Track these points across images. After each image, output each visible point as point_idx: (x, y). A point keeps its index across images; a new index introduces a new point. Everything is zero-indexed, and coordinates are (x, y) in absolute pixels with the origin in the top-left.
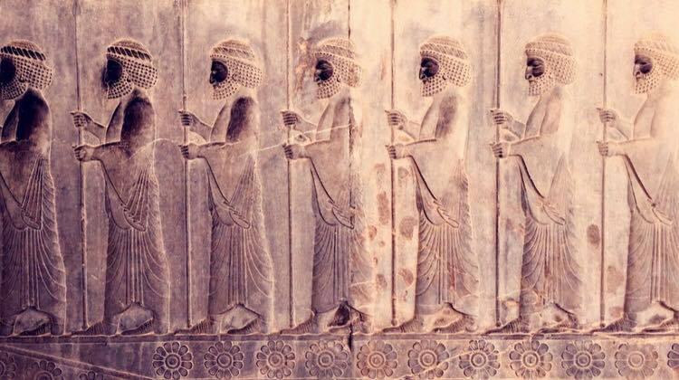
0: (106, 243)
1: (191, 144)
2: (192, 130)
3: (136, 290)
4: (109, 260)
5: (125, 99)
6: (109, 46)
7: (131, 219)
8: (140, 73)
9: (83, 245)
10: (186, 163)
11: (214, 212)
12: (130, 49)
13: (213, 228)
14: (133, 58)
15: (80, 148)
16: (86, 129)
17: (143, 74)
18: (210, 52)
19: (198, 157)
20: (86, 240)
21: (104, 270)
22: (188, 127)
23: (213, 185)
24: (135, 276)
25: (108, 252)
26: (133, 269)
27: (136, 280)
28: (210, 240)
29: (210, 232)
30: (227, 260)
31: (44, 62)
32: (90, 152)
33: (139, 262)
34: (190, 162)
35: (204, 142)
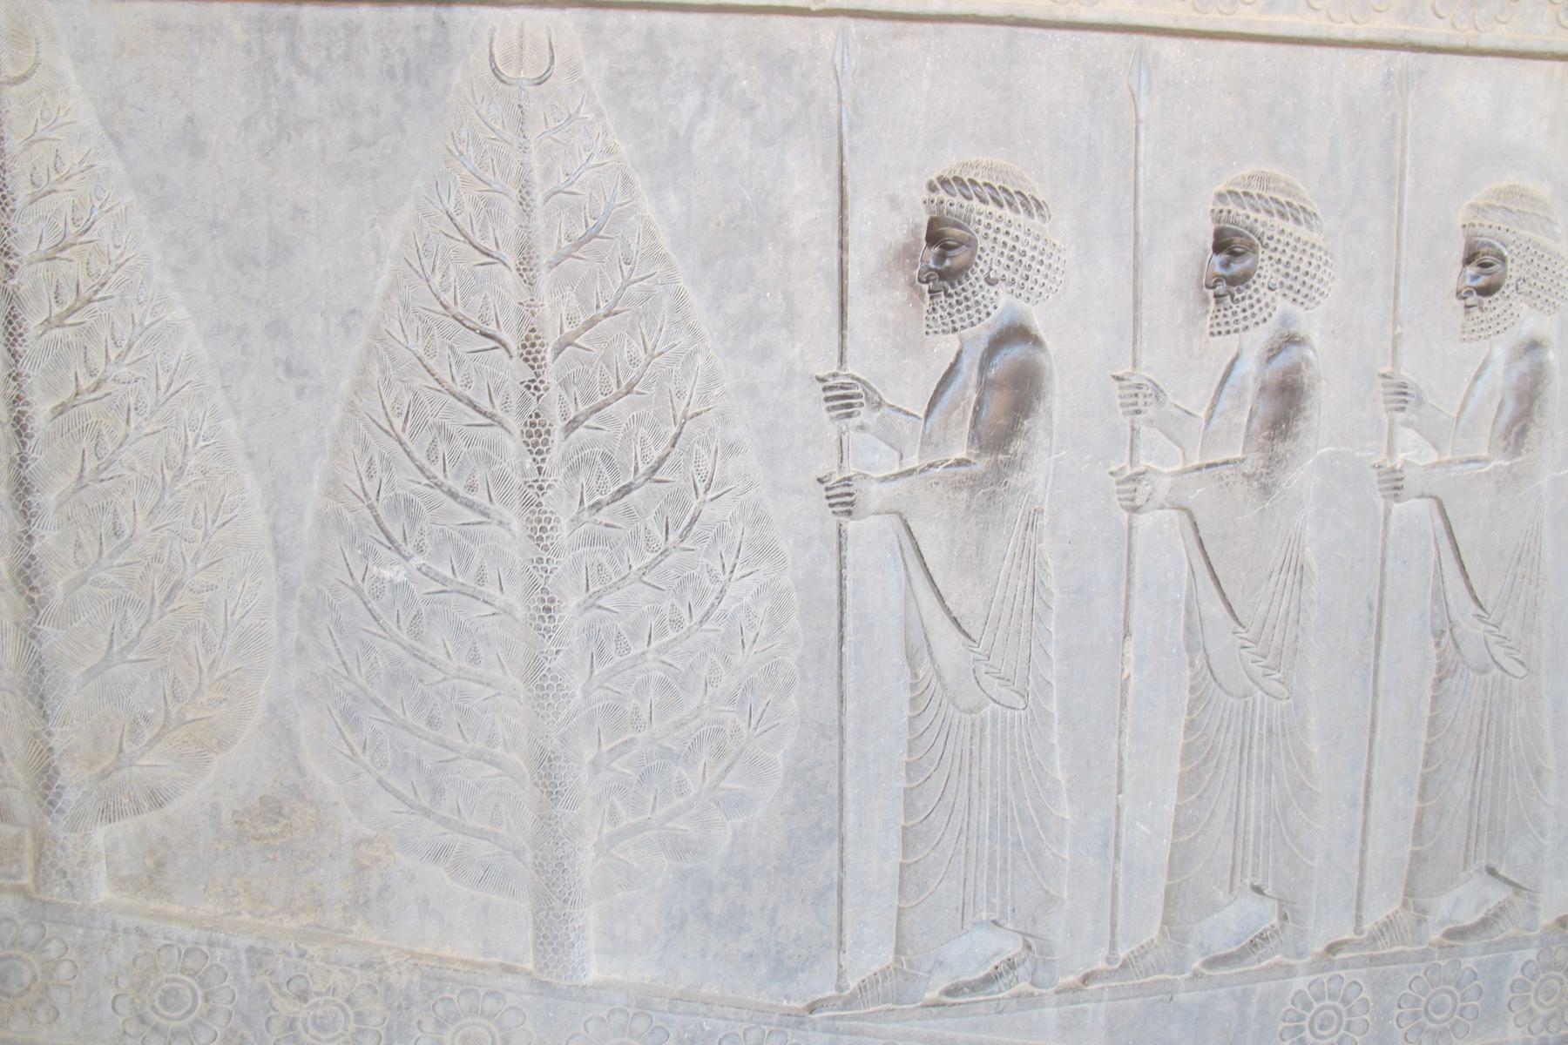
0: (1179, 738)
1: (1406, 463)
2: (1407, 424)
3: (1256, 855)
4: (1186, 784)
5: (1258, 338)
6: (1220, 188)
7: (1257, 670)
8: (1304, 267)
9: (1120, 745)
10: (1388, 512)
11: (1447, 638)
12: (1283, 199)
13: (1440, 680)
14: (1289, 226)
15: (1134, 478)
16: (1151, 422)
17: (1312, 270)
18: (1460, 216)
19: (1422, 496)
20: (1128, 730)
21: (1169, 808)
22: (1400, 416)
23: (1450, 567)
24: (1257, 818)
25: (1184, 760)
26: (1253, 801)
27: (1258, 829)
28: (1427, 712)
29: (1429, 693)
30: (1469, 762)
31: (1046, 226)
32: (1163, 487)
33: (1269, 782)
34: (1396, 507)
35: (1434, 458)
